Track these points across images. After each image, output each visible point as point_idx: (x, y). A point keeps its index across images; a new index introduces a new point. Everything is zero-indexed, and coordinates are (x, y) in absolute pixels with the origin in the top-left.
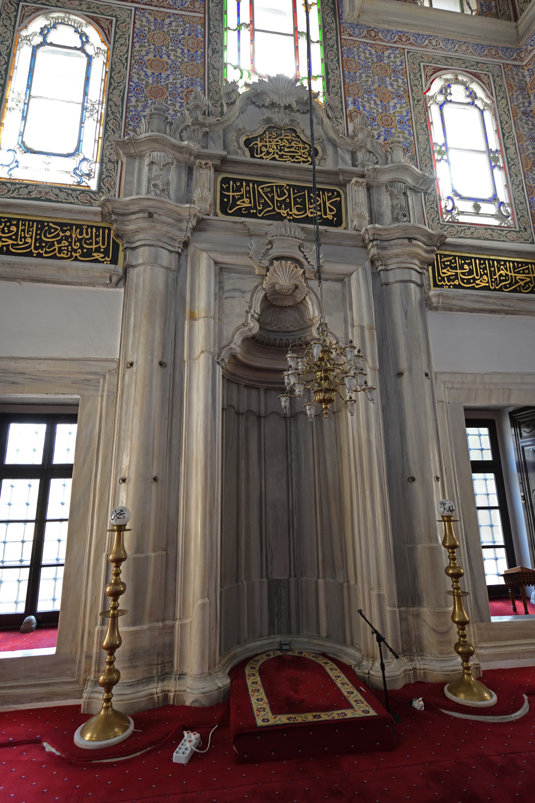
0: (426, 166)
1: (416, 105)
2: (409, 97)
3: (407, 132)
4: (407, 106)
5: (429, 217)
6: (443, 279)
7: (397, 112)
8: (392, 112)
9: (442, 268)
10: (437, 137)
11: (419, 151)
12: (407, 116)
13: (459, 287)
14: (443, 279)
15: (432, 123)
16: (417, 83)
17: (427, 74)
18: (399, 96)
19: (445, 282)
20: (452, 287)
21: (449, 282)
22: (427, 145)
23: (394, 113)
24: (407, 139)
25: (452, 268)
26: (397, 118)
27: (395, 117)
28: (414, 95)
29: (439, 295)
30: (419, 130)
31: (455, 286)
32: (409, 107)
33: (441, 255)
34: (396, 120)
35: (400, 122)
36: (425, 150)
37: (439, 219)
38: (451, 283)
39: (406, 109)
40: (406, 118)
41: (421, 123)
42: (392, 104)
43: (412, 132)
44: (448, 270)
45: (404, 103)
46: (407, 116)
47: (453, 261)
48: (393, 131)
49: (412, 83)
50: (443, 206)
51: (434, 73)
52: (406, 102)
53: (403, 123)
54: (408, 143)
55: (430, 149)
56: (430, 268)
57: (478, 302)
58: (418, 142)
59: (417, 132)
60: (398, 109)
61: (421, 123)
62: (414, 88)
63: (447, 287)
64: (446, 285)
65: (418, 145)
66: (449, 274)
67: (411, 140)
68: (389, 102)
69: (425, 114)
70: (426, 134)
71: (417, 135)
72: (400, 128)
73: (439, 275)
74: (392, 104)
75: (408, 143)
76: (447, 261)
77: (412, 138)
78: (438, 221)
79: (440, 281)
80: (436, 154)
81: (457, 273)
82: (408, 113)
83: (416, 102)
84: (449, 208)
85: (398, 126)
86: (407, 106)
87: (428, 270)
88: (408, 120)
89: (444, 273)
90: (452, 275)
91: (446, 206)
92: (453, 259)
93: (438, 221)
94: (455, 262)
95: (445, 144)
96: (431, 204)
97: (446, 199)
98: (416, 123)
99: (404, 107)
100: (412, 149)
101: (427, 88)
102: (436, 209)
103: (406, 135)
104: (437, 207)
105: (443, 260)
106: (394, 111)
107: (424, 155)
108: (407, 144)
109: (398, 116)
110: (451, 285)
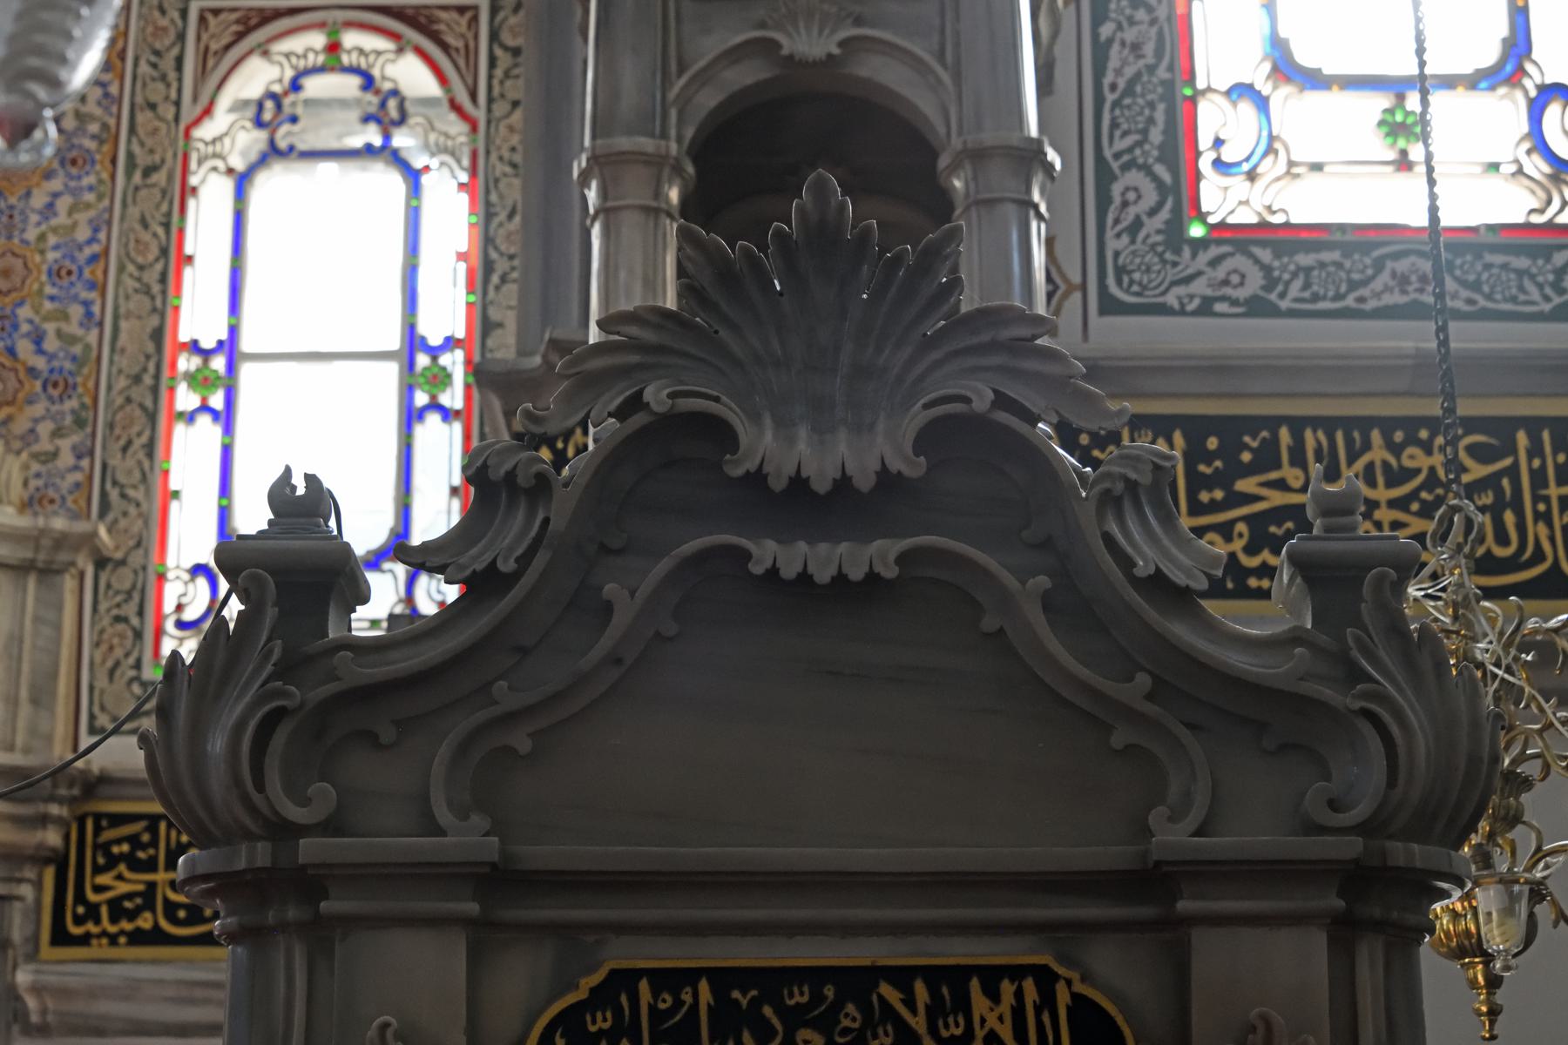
0: (129, 443)
1: (137, 189)
2: (114, 161)
3: (76, 311)
4: (100, 197)
5: (98, 659)
6: (93, 913)
7: (55, 230)
8: (31, 234)
9: (98, 870)
10: (199, 314)
11: (109, 388)
12: (91, 241)
13: (156, 937)
14: (93, 913)
15: (190, 259)
16: (156, 91)
17: (207, 49)
18: (74, 162)
19: (98, 921)
20: (122, 940)
21: (114, 920)
22: (148, 357)
23: (42, 237)
24: (73, 340)
25: (136, 866)
26: (51, 256)
27: (42, 252)
28: (136, 149)
29: (37, 989)
30: (127, 297)
31: (137, 938)
32: (106, 202)
33: (98, 817)
34: (45, 268)
35: (56, 273)
36: (137, 379)
37: (138, 665)
38: (127, 926)
39: (92, 213)
40: (88, 251)
41: (141, 268)
42: (39, 200)
43: (96, 309)
44: (120, 877)
45: (91, 188)
46: (91, 241)
47: (146, 838)
48: (24, 312)
49: (139, 99)
50: (169, 606)
51: (240, 36)
52: (100, 181)
53: (69, 273)
54: (74, 359)
55: (157, 377)
56: (49, 874)
57: (192, 1002)
58: (113, 350)
59: (116, 308)
60: (61, 219)
61: (141, 268)
62: (143, 117)
63: (105, 941)
64: (104, 933)
65: (111, 362)
66: (123, 888)
67: (87, 347)
68: (28, 194)
69: (167, 226)
70: (154, 310)
71: (116, 317)
72: (52, 298)
73: (80, 897)
74: (39, 200)
75: (74, 359)
76: (119, 841)
77: (92, 338)
78: (132, 673)
79: (79, 921)
80: (182, 389)
81: (152, 886)
82: (96, 230)
83: (137, 178)
84: (190, 615)
85: (49, 290)
86: (100, 197)
87: (38, 885)
88: (94, 258)
89: (99, 889)
90: (130, 896)
91: (180, 608)
92: (147, 829)
93: (132, 673)
94: (154, 843)
95: (230, 346)
96: (118, 606)
97: (186, 577)
98: (121, 269)
99: (88, 206)
100: (84, 385)
101: (198, 110)
102: (135, 621)
103: (73, 328)
104: (141, 613)
105: (107, 835)
106: (43, 227)
107: (129, 400)
108: (68, 365)
109: (56, 247)
110: (122, 932)
